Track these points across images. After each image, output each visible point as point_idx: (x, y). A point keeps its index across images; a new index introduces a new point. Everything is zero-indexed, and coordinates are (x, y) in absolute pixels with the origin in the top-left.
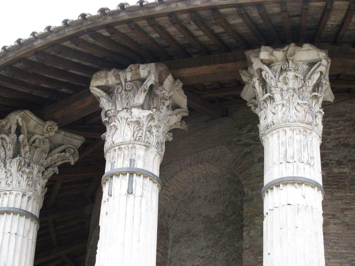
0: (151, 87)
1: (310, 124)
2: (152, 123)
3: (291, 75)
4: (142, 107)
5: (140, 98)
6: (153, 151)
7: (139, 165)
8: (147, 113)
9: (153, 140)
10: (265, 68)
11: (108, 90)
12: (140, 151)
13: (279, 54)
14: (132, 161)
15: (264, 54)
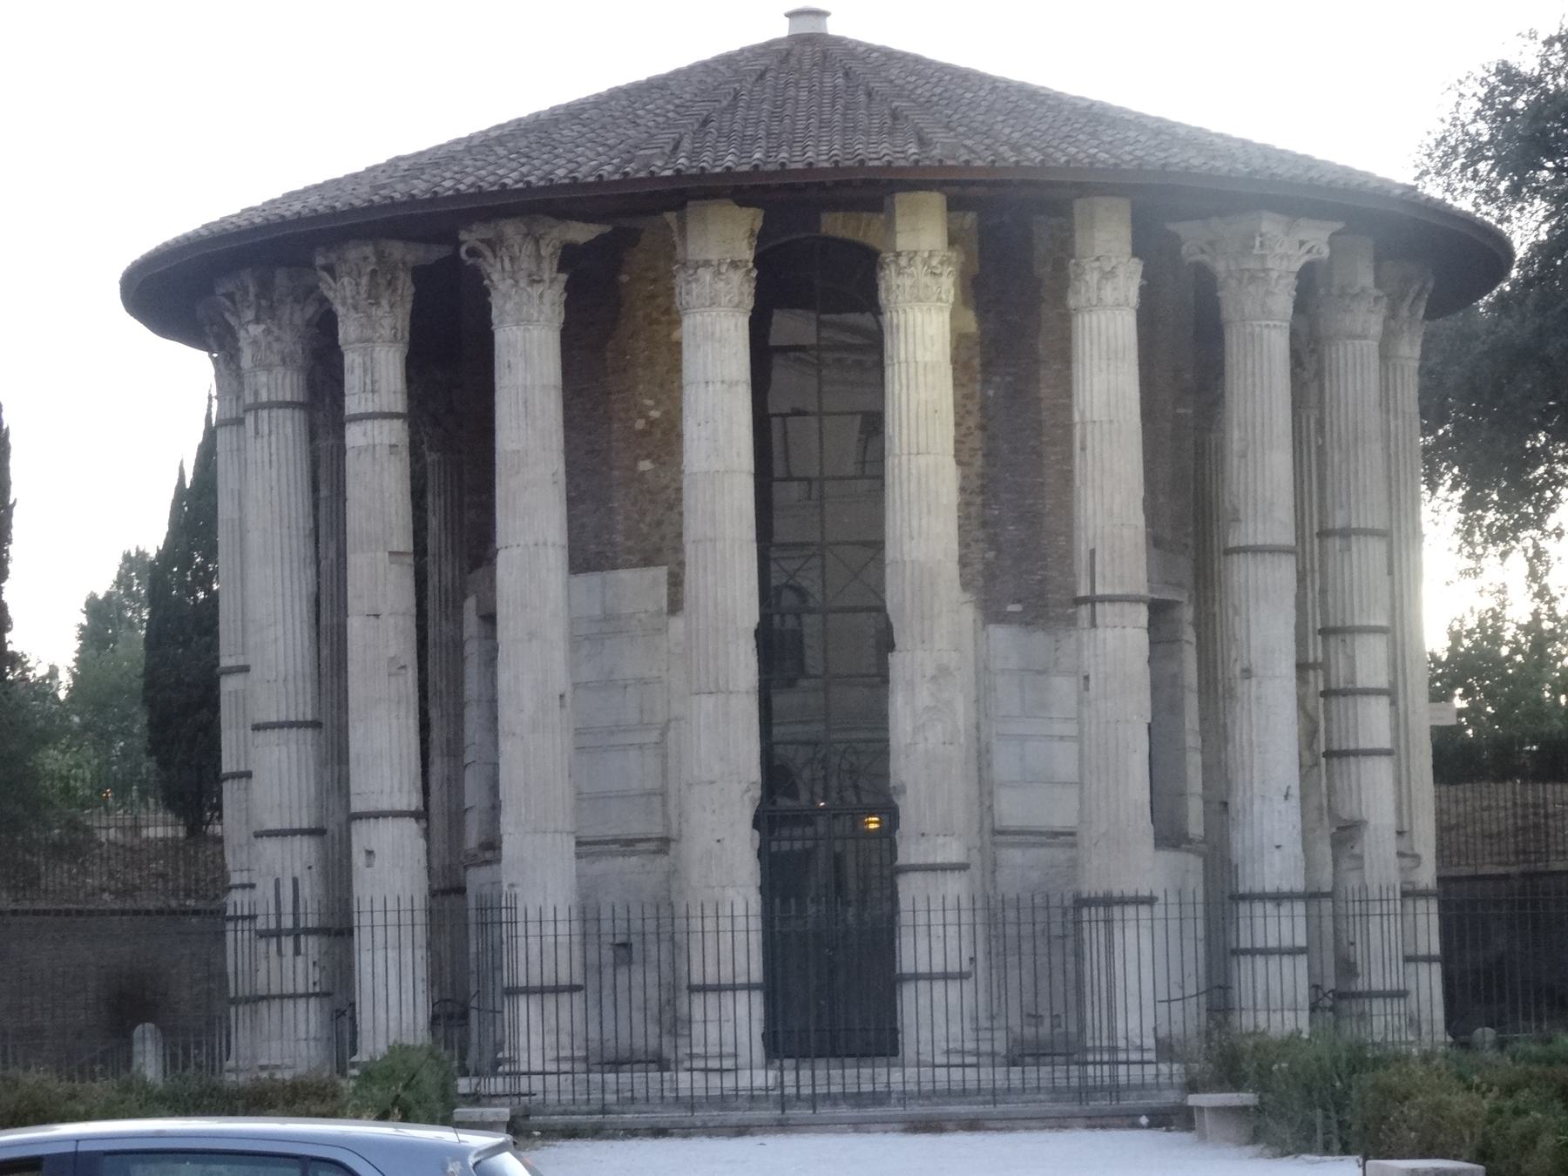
0: (257, 296)
1: (368, 340)
2: (270, 338)
3: (346, 280)
4: (257, 320)
5: (249, 315)
6: (279, 372)
7: (264, 397)
8: (263, 327)
9: (276, 359)
10: (325, 275)
11: (230, 296)
12: (263, 378)
13: (333, 257)
14: (256, 393)
15: (320, 261)
